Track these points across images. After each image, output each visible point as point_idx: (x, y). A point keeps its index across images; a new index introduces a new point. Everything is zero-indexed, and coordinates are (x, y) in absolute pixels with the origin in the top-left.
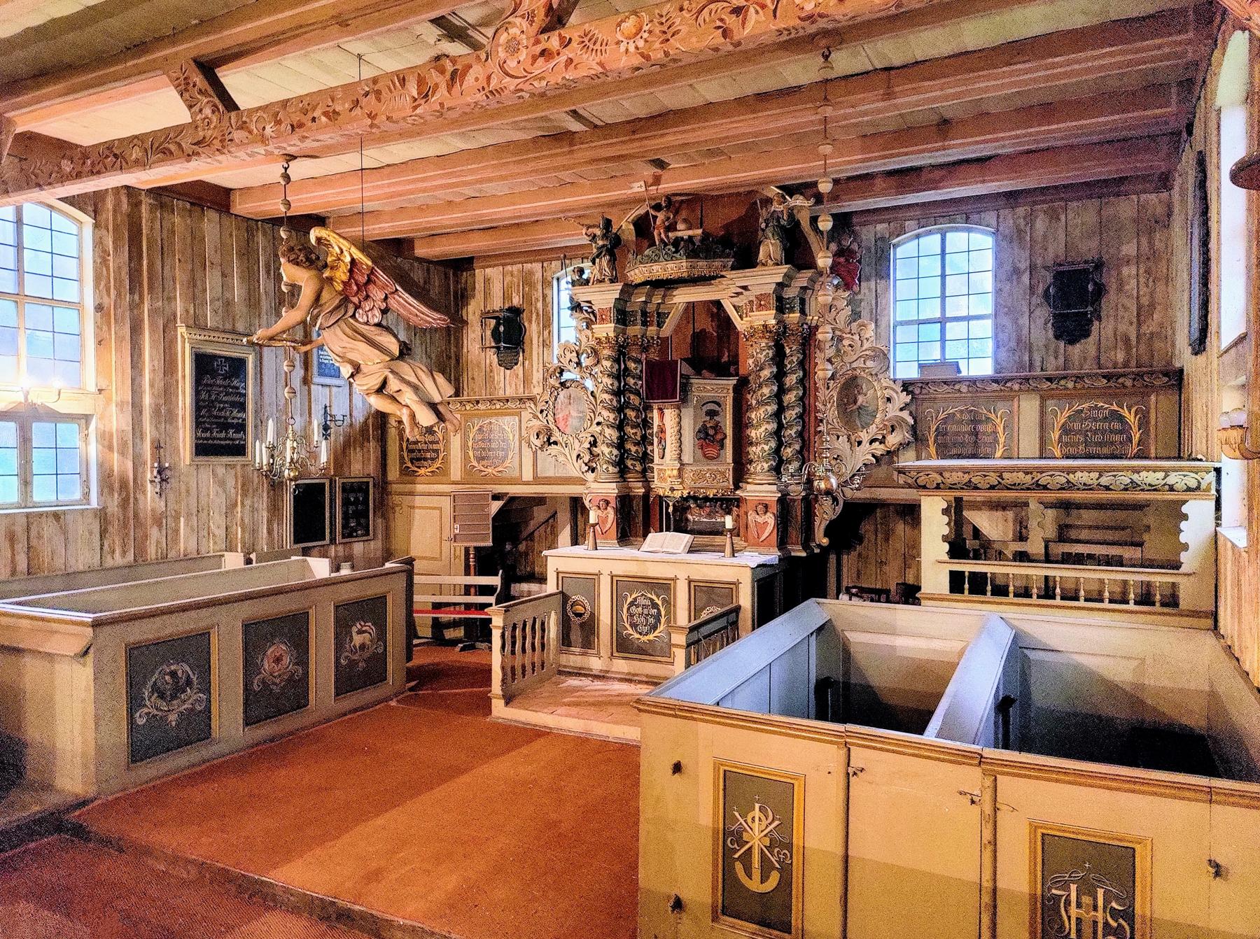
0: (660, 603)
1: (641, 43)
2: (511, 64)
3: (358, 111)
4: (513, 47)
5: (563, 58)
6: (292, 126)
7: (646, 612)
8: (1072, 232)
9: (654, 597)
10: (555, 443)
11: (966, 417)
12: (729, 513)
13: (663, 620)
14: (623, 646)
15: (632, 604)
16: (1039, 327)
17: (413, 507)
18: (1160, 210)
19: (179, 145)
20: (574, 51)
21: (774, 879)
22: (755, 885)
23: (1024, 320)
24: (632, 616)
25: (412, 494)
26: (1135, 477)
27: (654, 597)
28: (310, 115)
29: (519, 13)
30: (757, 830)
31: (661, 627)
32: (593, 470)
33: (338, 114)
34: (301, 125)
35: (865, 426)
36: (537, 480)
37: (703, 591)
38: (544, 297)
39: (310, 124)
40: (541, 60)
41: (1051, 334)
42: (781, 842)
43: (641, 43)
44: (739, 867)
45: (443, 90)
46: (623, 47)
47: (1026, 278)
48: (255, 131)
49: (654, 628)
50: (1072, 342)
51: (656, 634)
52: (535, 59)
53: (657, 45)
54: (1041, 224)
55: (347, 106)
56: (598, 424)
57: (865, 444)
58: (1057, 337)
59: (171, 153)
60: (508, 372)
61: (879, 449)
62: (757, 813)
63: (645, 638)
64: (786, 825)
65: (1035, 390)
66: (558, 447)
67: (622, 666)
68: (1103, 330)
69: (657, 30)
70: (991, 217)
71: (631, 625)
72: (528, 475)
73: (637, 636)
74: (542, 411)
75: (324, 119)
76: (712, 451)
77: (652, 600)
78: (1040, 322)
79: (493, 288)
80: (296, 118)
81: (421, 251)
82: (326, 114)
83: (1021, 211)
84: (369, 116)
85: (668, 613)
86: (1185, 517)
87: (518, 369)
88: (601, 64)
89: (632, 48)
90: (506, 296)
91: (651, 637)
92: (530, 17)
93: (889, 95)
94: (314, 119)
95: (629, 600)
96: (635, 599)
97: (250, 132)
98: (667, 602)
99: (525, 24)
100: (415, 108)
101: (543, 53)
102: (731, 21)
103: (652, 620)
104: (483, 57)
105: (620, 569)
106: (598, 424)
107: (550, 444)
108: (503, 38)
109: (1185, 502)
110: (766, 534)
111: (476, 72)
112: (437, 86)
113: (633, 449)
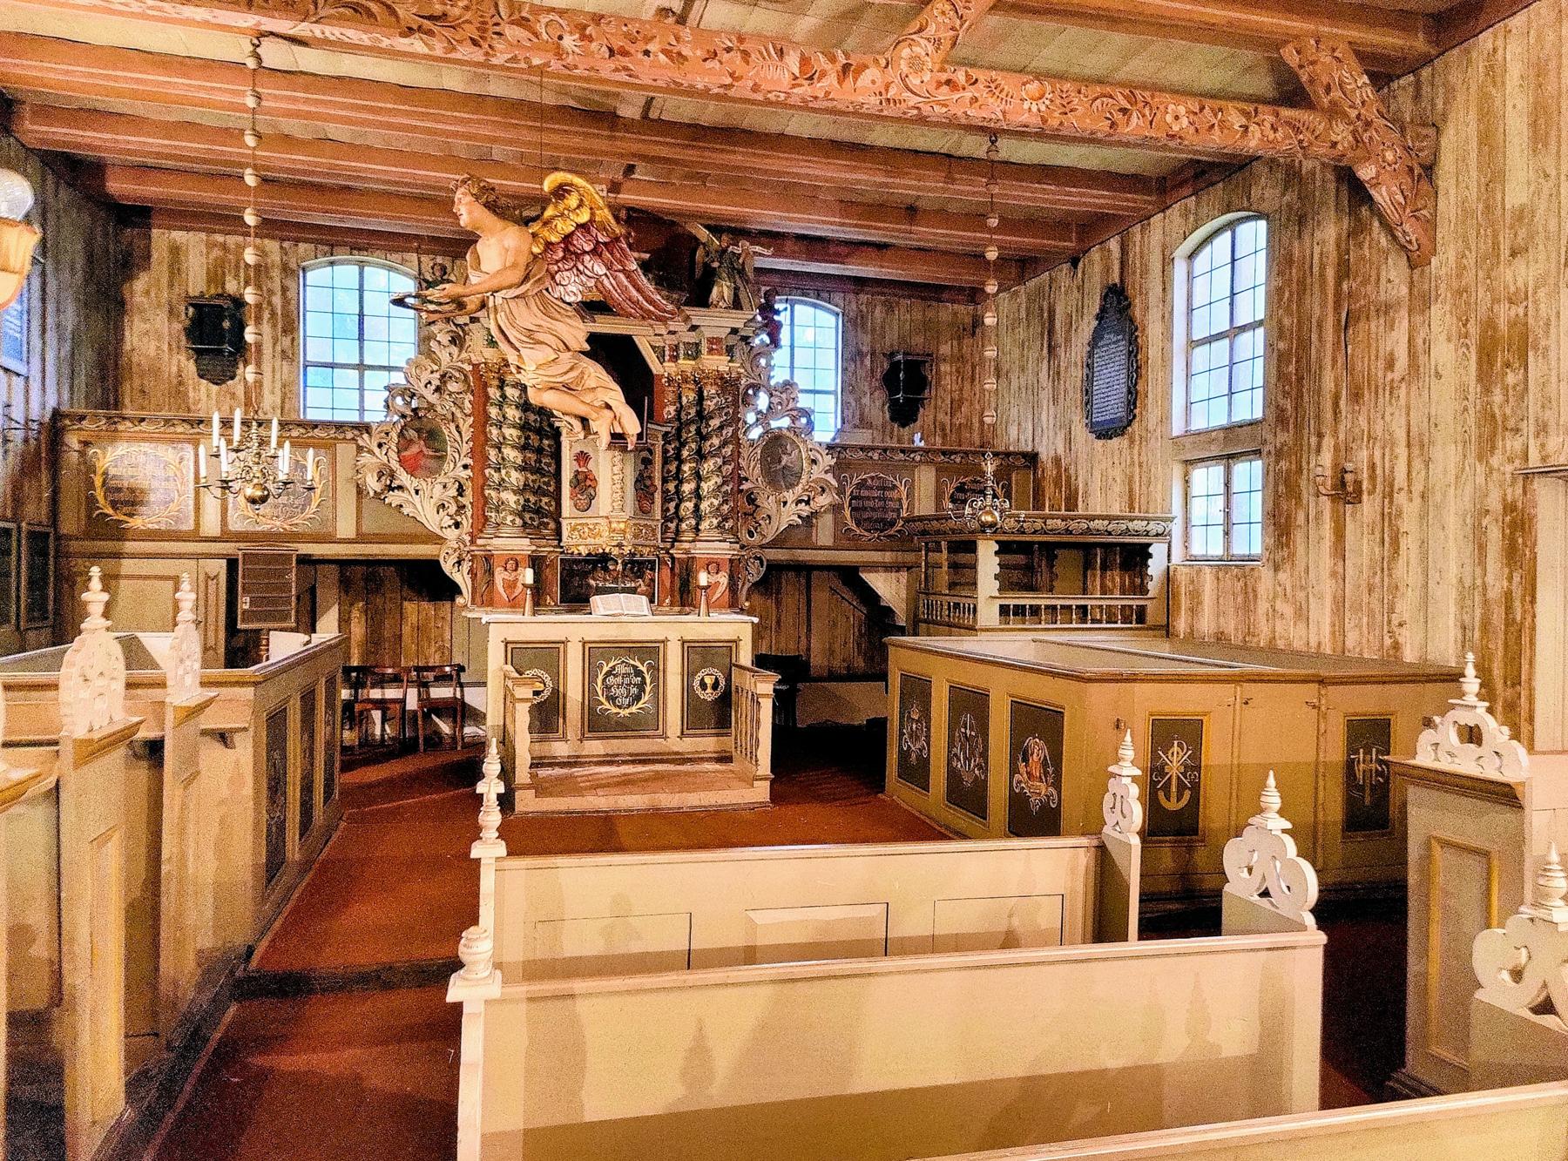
0: (644, 669)
1: (1043, 108)
2: (914, 81)
3: (713, 64)
4: (916, 63)
5: (968, 95)
6: (611, 50)
7: (627, 681)
8: (900, 325)
9: (637, 664)
10: (400, 488)
11: (877, 483)
12: (641, 577)
13: (648, 689)
14: (596, 724)
15: (609, 673)
16: (876, 406)
17: (117, 577)
18: (968, 320)
19: (393, 12)
20: (980, 91)
21: (1187, 794)
22: (1173, 805)
23: (866, 400)
24: (608, 688)
25: (118, 556)
26: (1131, 525)
27: (637, 664)
28: (642, 46)
29: (923, 34)
30: (1175, 760)
31: (646, 698)
32: (457, 525)
33: (685, 58)
34: (624, 53)
35: (791, 486)
36: (361, 538)
37: (699, 653)
38: (284, 289)
39: (640, 56)
40: (945, 89)
41: (887, 415)
42: (1194, 766)
43: (1043, 108)
44: (1161, 795)
45: (831, 80)
46: (1026, 105)
47: (868, 362)
48: (545, 36)
49: (638, 698)
50: (903, 425)
51: (640, 705)
52: (939, 84)
53: (1056, 114)
54: (879, 312)
55: (699, 53)
56: (465, 467)
57: (791, 507)
58: (893, 419)
59: (370, 14)
60: (215, 388)
61: (805, 510)
62: (1176, 748)
63: (624, 713)
64: (1196, 756)
65: (932, 462)
66: (405, 495)
67: (596, 747)
68: (925, 415)
69: (1058, 101)
70: (838, 297)
71: (608, 698)
72: (346, 528)
73: (615, 710)
74: (380, 446)
75: (662, 57)
76: (646, 504)
77: (635, 667)
78: (878, 403)
79: (185, 261)
80: (617, 43)
81: (117, 186)
82: (664, 51)
83: (863, 298)
84: (731, 75)
85: (655, 679)
86: (1150, 556)
87: (236, 386)
88: (1004, 113)
89: (1034, 109)
90: (216, 277)
91: (634, 709)
92: (937, 43)
93: (950, 179)
94: (647, 53)
95: (606, 669)
96: (613, 668)
97: (536, 35)
98: (654, 669)
99: (930, 48)
100: (794, 86)
101: (948, 82)
102: (1118, 116)
103: (634, 690)
104: (883, 63)
105: (595, 633)
106: (465, 467)
107: (390, 488)
108: (906, 52)
109: (1149, 545)
110: (718, 595)
111: (871, 74)
112: (823, 74)
113: (532, 499)
